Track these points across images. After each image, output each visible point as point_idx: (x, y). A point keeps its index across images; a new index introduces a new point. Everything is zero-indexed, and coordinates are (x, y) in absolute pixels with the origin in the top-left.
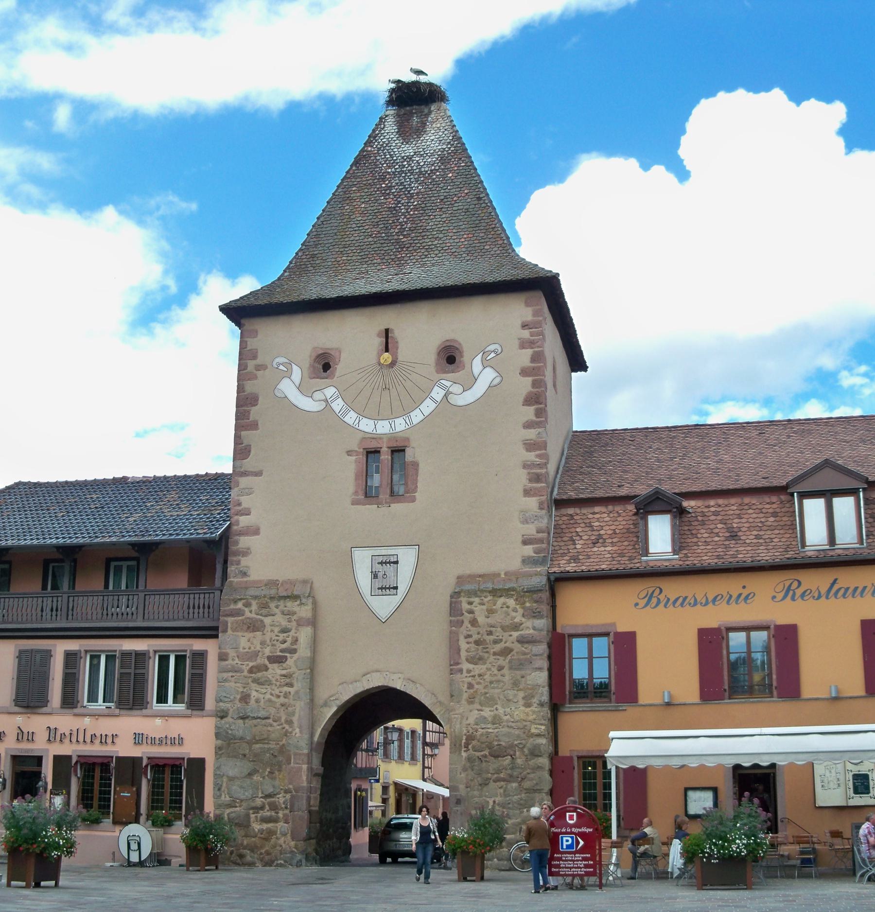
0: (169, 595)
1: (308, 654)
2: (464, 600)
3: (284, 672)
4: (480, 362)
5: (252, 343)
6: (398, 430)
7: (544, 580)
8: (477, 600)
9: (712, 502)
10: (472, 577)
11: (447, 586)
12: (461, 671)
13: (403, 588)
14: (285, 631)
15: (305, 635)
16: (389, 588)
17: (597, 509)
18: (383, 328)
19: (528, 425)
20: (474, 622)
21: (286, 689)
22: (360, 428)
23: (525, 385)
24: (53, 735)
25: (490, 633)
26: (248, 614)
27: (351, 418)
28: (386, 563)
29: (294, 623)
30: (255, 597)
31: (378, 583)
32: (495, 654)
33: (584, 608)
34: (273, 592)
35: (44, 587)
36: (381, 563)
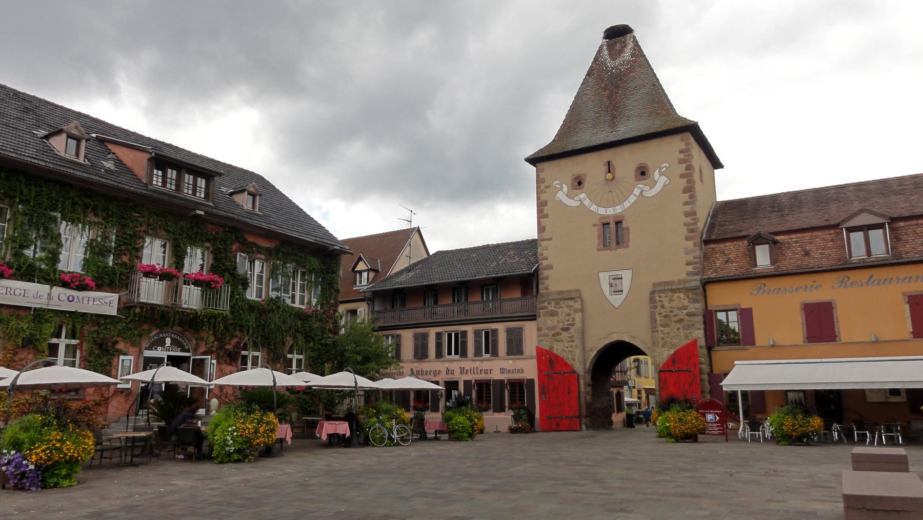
0: (512, 300)
1: (580, 326)
2: (657, 295)
5: (542, 175)
7: (698, 283)
8: (663, 295)
9: (794, 236)
10: (660, 284)
11: (649, 288)
15: (578, 316)
17: (727, 244)
18: (606, 161)
19: (686, 204)
20: (663, 306)
23: (683, 182)
24: (463, 371)
25: (672, 312)
27: (594, 208)
31: (613, 289)
34: (561, 296)
35: (454, 301)
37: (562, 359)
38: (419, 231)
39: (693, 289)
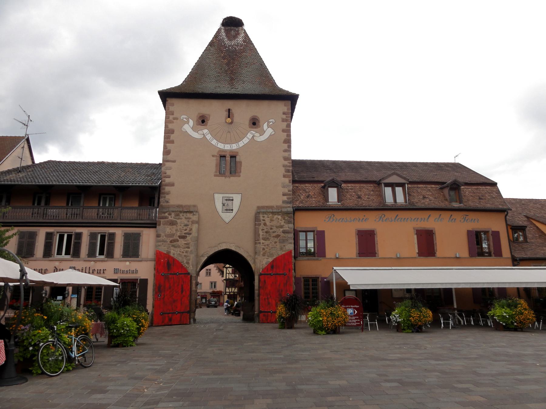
0: (131, 210)
2: (261, 216)
3: (186, 242)
8: (266, 216)
9: (349, 185)
10: (263, 207)
12: (260, 243)
13: (235, 210)
14: (186, 225)
17: (307, 185)
18: (228, 108)
20: (265, 224)
21: (186, 249)
25: (271, 229)
26: (170, 218)
27: (214, 142)
29: (190, 223)
30: (173, 211)
31: (225, 208)
32: (273, 237)
33: (306, 221)
34: (181, 210)
35: (68, 204)
36: (226, 200)
37: (178, 261)
38: (28, 140)
39: (287, 213)
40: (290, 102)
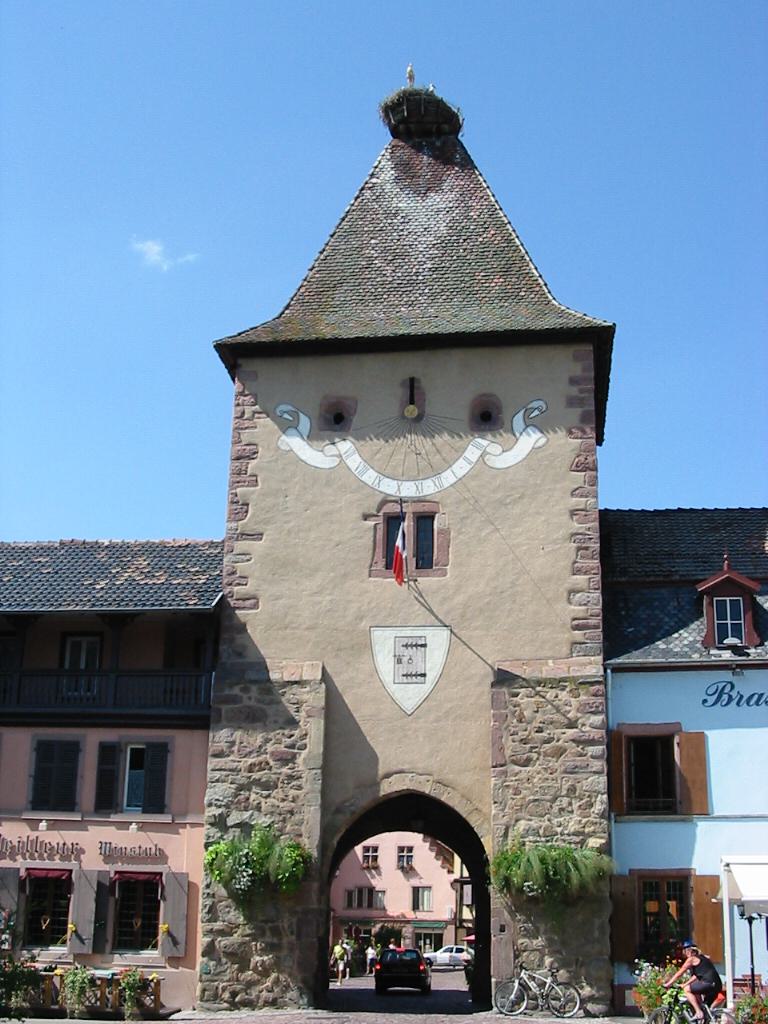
4: (521, 422)
6: (425, 493)
13: (431, 677)
16: (416, 675)
22: (380, 489)
25: (540, 730)
26: (246, 702)
27: (370, 477)
28: (412, 646)
30: (255, 682)
31: (404, 669)
36: (406, 646)
40: (591, 348)
